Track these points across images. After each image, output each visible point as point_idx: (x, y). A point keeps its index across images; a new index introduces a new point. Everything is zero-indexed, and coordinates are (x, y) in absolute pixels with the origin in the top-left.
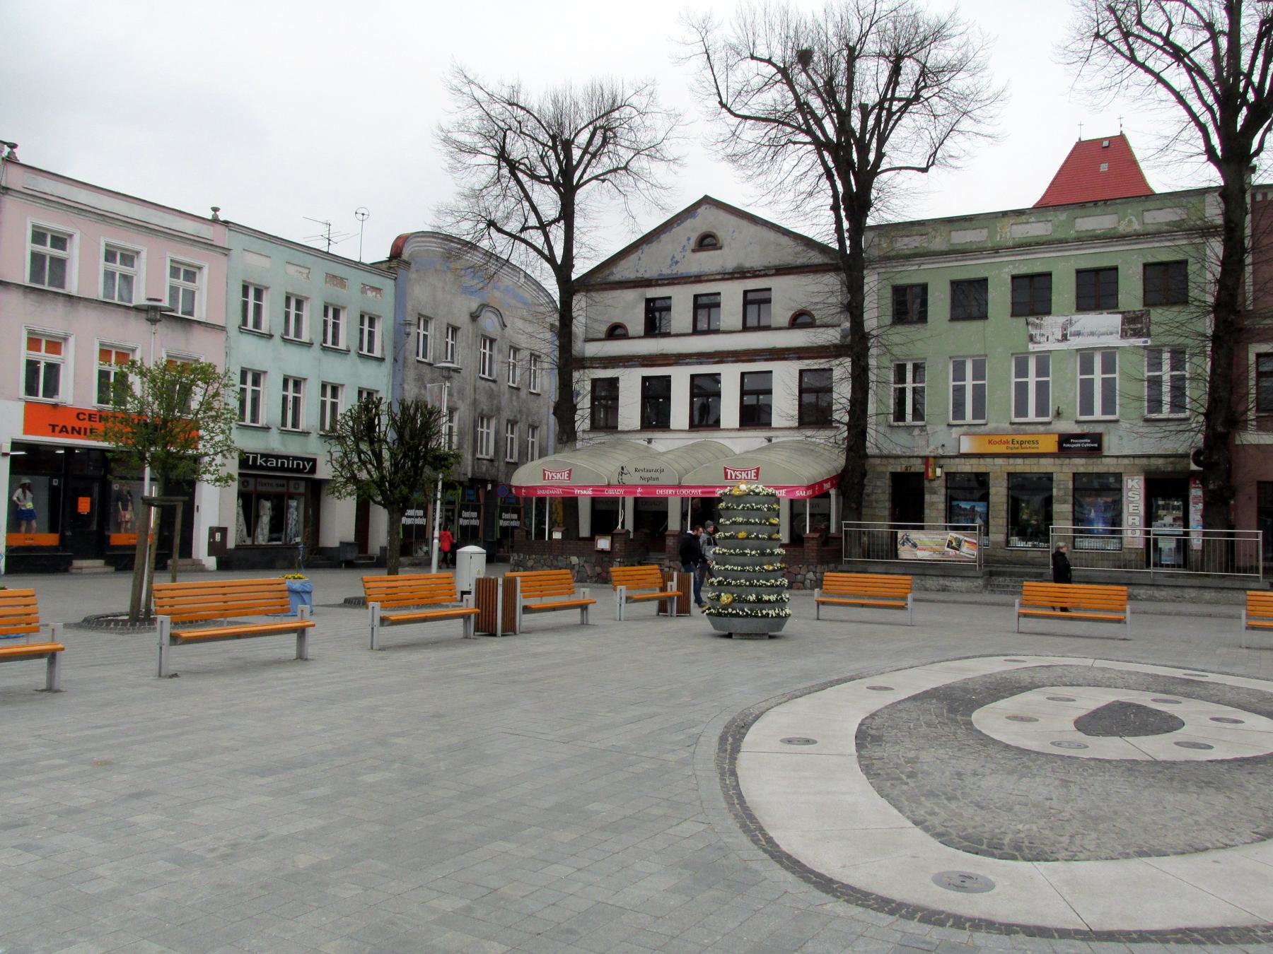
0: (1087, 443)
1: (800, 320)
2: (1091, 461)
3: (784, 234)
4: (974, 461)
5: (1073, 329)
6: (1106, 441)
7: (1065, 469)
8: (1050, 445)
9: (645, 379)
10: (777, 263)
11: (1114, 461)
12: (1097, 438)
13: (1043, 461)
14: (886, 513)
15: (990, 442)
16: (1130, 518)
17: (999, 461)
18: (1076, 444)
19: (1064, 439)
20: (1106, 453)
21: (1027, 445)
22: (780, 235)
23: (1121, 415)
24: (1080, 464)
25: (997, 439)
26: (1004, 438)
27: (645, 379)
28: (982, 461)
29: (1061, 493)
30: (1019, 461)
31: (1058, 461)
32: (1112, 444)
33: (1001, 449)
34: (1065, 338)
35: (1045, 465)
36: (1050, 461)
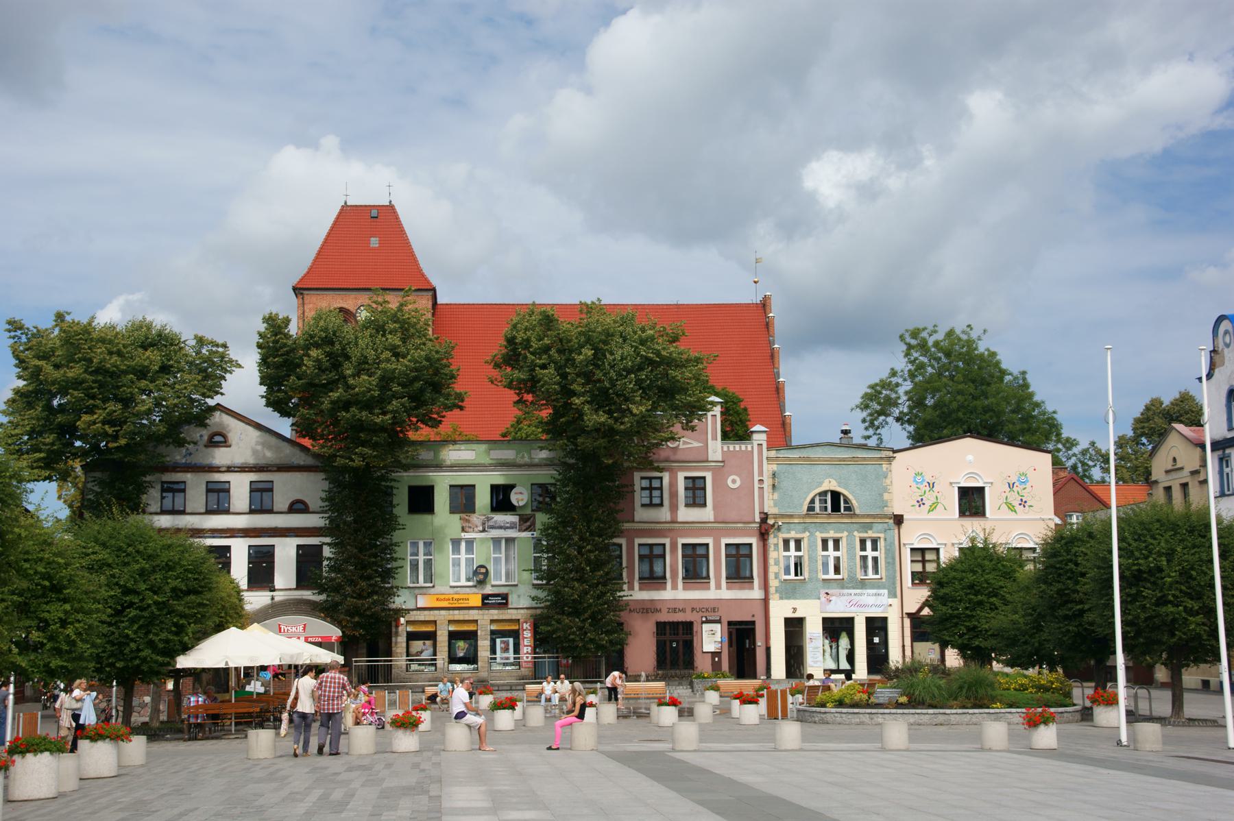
0: (499, 600)
1: (298, 507)
2: (501, 611)
3: (283, 440)
4: (426, 612)
5: (491, 523)
6: (510, 599)
7: (486, 617)
8: (477, 601)
9: (299, 547)
10: (278, 462)
11: (514, 611)
12: (505, 597)
13: (471, 612)
14: (364, 651)
15: (437, 599)
16: (525, 648)
17: (443, 612)
18: (492, 601)
19: (485, 597)
20: (510, 606)
21: (462, 601)
22: (281, 441)
23: (518, 581)
24: (495, 614)
25: (442, 597)
26: (447, 597)
27: (299, 547)
28: (432, 612)
29: (483, 633)
30: (456, 612)
31: (481, 612)
32: (513, 600)
33: (445, 604)
34: (484, 531)
35: (473, 615)
36: (475, 612)
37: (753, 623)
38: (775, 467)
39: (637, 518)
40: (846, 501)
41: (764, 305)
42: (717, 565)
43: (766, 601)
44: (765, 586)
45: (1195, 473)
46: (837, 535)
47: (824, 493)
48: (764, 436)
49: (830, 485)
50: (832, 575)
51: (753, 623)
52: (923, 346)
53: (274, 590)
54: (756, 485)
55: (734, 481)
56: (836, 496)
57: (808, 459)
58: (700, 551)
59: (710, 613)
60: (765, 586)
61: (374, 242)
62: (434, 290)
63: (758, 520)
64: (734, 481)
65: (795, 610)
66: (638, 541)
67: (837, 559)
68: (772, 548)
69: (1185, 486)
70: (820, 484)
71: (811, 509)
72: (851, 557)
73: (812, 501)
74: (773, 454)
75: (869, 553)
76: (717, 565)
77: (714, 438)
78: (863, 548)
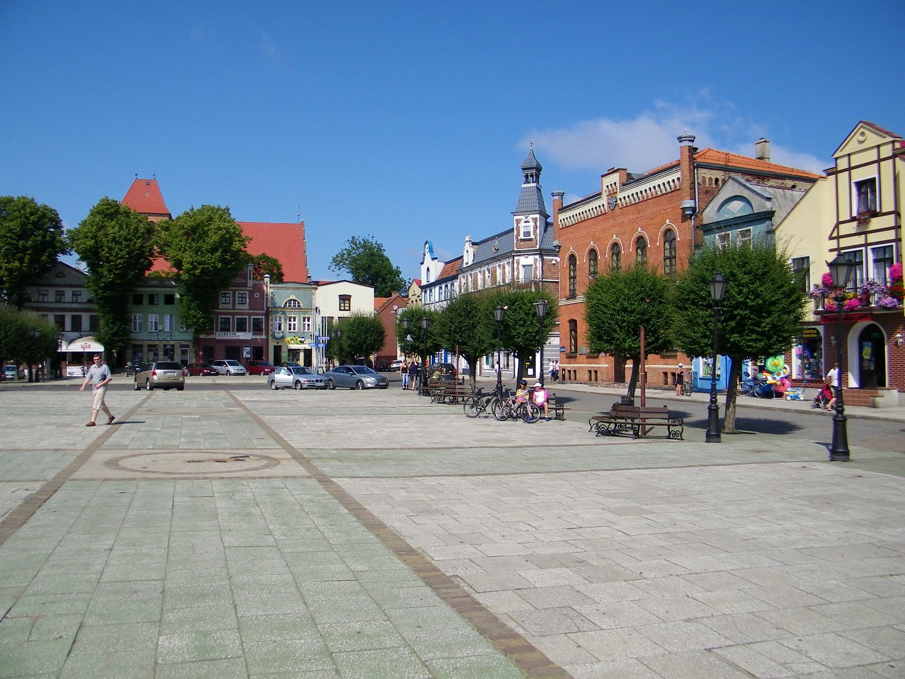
37: (262, 347)
38: (272, 290)
39: (220, 307)
40: (299, 303)
41: (302, 224)
42: (249, 324)
43: (267, 340)
44: (267, 334)
45: (419, 296)
46: (295, 316)
47: (291, 300)
48: (269, 279)
49: (293, 297)
50: (292, 330)
51: (262, 347)
52: (355, 244)
53: (81, 331)
54: (265, 297)
55: (257, 295)
56: (295, 301)
57: (285, 288)
58: (244, 321)
59: (245, 342)
60: (267, 334)
61: (147, 194)
62: (170, 214)
63: (265, 309)
64: (257, 295)
65: (278, 343)
66: (220, 316)
67: (294, 324)
68: (270, 320)
69: (416, 300)
70: (289, 297)
71: (285, 305)
72: (299, 323)
73: (286, 303)
74: (272, 285)
75: (306, 322)
76: (249, 324)
77: (250, 279)
78: (304, 321)
